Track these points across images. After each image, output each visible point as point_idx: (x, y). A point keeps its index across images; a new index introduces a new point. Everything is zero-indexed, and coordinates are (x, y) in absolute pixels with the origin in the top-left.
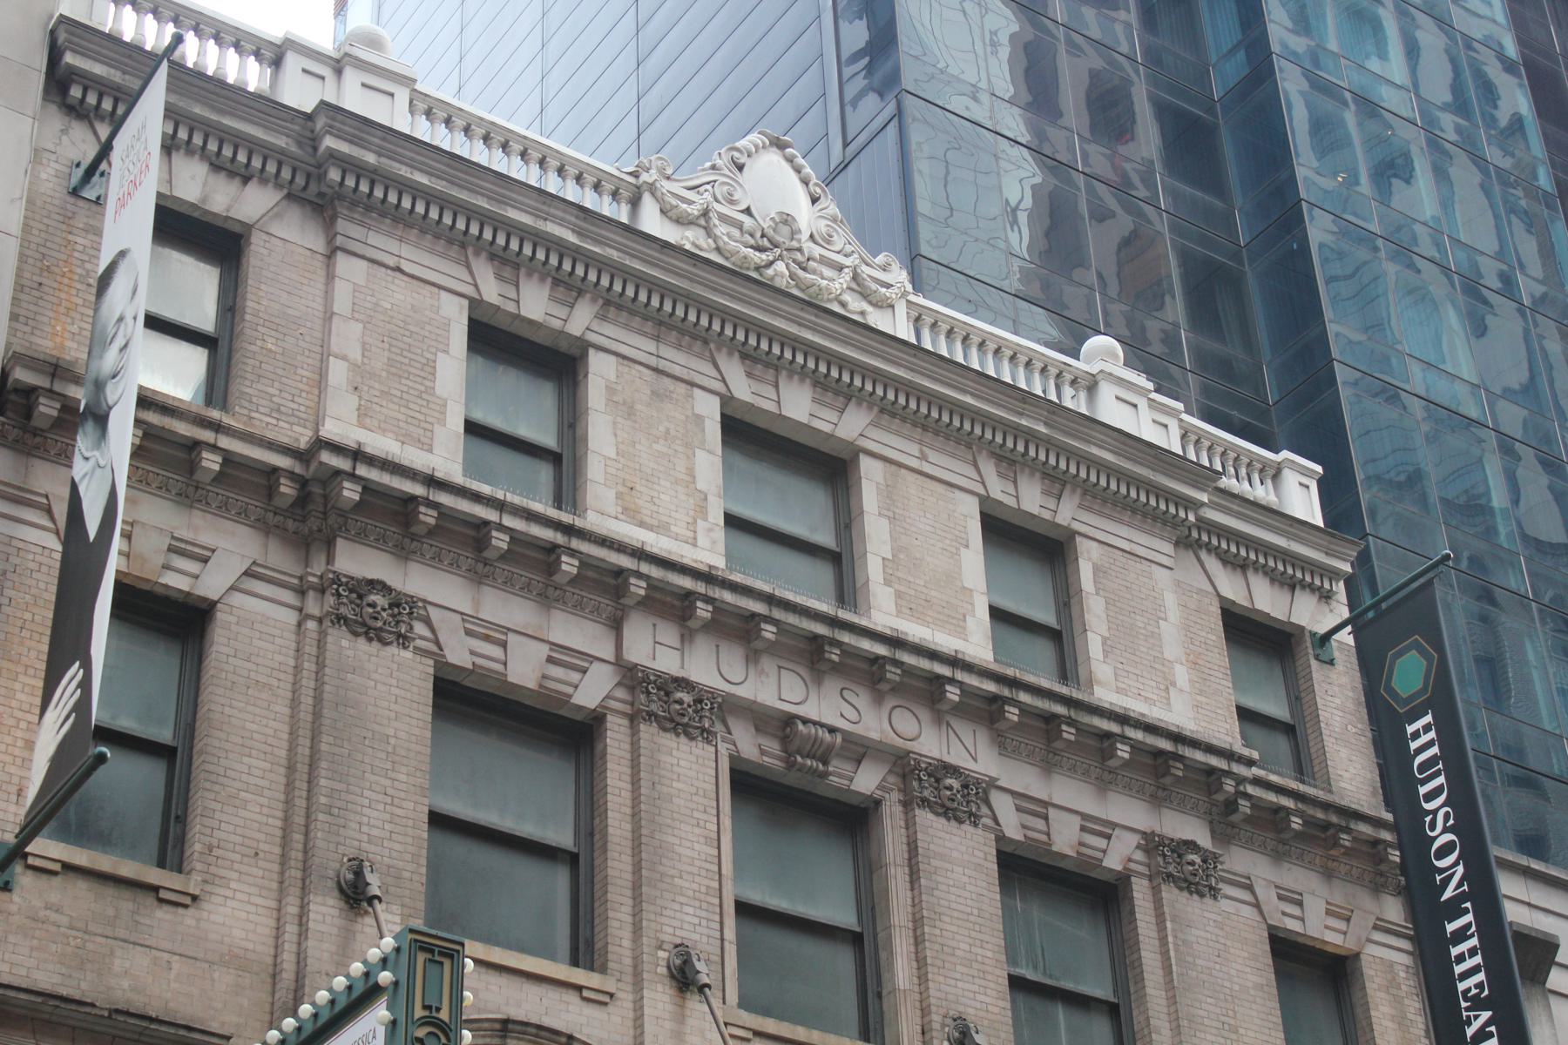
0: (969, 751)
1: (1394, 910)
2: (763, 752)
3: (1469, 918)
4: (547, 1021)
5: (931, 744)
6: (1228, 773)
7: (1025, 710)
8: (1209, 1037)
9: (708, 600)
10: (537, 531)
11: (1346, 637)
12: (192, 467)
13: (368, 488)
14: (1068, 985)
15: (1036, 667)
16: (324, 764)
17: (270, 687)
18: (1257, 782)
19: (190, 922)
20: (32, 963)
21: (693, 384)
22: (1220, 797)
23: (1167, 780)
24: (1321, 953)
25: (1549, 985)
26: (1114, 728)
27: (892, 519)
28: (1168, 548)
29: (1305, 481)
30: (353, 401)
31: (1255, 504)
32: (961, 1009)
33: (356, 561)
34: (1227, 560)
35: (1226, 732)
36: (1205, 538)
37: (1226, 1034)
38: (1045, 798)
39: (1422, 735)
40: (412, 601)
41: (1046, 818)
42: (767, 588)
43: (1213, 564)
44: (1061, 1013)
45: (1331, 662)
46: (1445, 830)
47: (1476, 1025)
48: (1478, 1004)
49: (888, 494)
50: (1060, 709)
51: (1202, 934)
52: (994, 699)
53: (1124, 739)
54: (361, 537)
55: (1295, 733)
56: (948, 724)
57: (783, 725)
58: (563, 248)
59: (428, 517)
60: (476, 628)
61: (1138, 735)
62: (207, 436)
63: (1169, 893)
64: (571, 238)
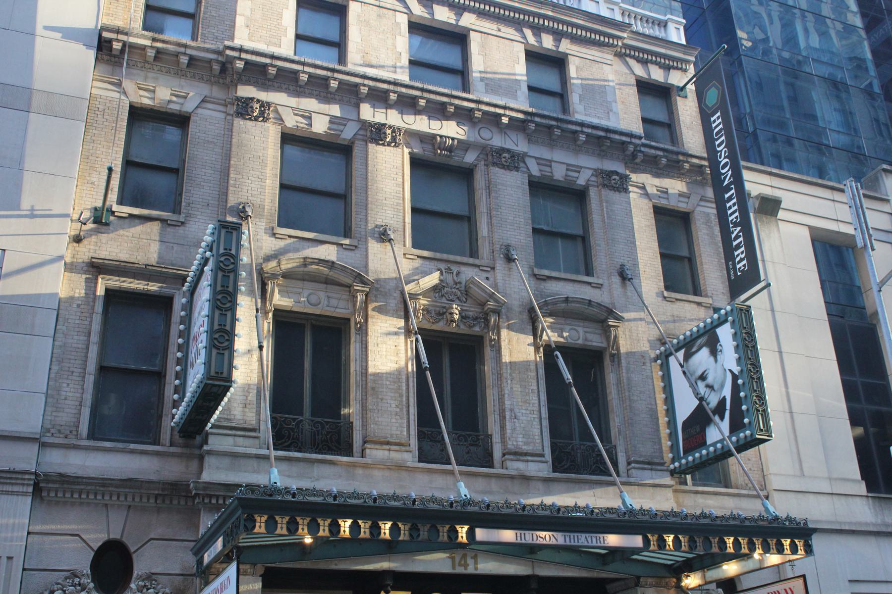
0: (517, 144)
1: (710, 193)
3: (733, 191)
4: (323, 258)
5: (497, 141)
6: (630, 143)
7: (537, 124)
9: (395, 92)
10: (319, 72)
11: (691, 87)
12: (178, 63)
13: (247, 62)
14: (564, 231)
15: (550, 107)
16: (232, 169)
17: (213, 142)
18: (644, 145)
20: (118, 251)
21: (395, 11)
22: (628, 153)
23: (604, 148)
24: (678, 212)
25: (778, 217)
26: (578, 128)
27: (485, 56)
28: (610, 57)
29: (678, 26)
30: (247, 31)
31: (649, 36)
33: (246, 91)
34: (639, 60)
35: (638, 128)
36: (628, 52)
38: (549, 158)
39: (717, 120)
40: (269, 104)
42: (420, 85)
43: (632, 62)
44: (559, 242)
45: (686, 97)
46: (725, 158)
47: (735, 233)
48: (736, 225)
49: (483, 46)
50: (554, 123)
52: (523, 121)
53: (582, 132)
54: (248, 83)
55: (670, 126)
59: (272, 71)
60: (296, 112)
61: (589, 131)
62: (182, 50)
63: (605, 192)
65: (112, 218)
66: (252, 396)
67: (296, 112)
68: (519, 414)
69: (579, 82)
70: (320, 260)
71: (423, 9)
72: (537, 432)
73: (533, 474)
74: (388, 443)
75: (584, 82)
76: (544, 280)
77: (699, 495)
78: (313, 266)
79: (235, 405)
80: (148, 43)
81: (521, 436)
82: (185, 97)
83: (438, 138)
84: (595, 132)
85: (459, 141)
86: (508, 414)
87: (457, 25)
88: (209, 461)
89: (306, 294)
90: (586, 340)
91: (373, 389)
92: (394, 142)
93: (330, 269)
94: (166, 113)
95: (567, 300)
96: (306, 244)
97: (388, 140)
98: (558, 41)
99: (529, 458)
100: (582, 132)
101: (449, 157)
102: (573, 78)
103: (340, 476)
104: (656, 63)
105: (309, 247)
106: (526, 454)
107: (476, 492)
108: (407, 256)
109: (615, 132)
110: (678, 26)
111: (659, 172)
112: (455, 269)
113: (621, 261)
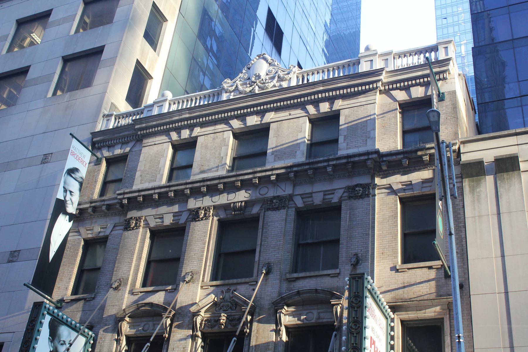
5: (271, 193)
8: (357, 240)
9: (204, 186)
13: (129, 199)
19: (92, 303)
25: (522, 169)
26: (326, 164)
32: (269, 261)
34: (401, 89)
37: (364, 237)
38: (310, 191)
40: (140, 218)
41: (312, 197)
50: (307, 167)
51: (361, 210)
57: (226, 207)
58: (187, 119)
60: (156, 217)
61: (334, 162)
62: (103, 203)
64: (187, 116)
65: (63, 304)
67: (156, 217)
69: (346, 125)
70: (145, 303)
71: (241, 123)
76: (294, 281)
78: (143, 308)
80: (87, 206)
82: (106, 228)
83: (232, 205)
84: (338, 162)
85: (246, 202)
87: (261, 124)
89: (143, 324)
90: (319, 318)
92: (206, 217)
94: (100, 239)
95: (298, 293)
96: (149, 294)
97: (201, 217)
98: (332, 104)
100: (329, 165)
101: (241, 214)
104: (416, 85)
105: (150, 296)
108: (204, 287)
109: (354, 156)
110: (446, 46)
112: (232, 288)
113: (354, 252)
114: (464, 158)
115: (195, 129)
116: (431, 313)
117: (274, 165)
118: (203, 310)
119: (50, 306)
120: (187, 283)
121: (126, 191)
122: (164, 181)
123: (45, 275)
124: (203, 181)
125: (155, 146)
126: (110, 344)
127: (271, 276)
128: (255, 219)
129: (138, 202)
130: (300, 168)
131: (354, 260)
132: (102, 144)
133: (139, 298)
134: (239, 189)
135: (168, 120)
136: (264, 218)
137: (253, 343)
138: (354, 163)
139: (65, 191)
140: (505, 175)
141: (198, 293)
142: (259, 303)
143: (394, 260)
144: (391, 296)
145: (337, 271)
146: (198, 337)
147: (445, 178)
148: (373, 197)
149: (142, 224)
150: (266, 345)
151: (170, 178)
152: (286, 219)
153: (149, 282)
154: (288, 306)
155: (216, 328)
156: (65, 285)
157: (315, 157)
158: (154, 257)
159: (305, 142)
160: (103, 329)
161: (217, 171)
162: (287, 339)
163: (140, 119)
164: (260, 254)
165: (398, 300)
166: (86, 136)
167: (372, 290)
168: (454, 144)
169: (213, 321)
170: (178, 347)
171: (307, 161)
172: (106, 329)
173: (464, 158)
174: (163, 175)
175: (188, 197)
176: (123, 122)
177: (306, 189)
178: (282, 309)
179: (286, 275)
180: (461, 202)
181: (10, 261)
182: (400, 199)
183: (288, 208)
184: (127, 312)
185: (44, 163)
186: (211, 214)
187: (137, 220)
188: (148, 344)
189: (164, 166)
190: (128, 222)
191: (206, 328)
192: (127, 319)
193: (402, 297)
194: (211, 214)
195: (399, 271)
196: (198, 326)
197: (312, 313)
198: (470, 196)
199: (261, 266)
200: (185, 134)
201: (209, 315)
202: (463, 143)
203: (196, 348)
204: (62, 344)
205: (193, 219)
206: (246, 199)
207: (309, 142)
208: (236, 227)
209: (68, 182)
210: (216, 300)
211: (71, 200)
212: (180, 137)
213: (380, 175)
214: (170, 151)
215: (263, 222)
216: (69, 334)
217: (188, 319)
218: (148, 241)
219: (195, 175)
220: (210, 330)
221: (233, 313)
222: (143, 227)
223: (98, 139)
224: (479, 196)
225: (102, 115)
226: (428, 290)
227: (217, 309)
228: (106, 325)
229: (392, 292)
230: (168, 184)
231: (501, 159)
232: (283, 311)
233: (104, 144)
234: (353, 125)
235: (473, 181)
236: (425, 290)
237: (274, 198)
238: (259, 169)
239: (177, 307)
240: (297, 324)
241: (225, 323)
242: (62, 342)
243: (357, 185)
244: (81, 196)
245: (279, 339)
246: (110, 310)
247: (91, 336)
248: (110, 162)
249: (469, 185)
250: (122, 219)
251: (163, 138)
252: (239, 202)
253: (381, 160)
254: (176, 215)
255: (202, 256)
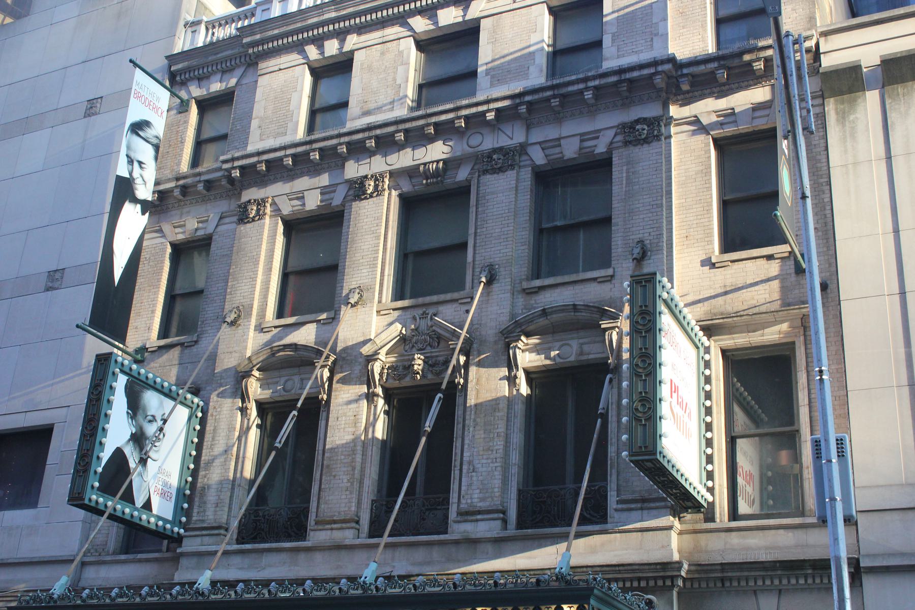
2: (414, 186)
5: (488, 142)
7: (530, 104)
8: (641, 217)
9: (370, 138)
13: (242, 168)
14: (585, 218)
19: (195, 350)
26: (581, 86)
38: (557, 136)
40: (264, 201)
41: (560, 146)
50: (549, 93)
51: (647, 163)
54: (250, 186)
56: (499, 129)
57: (411, 172)
60: (292, 196)
61: (597, 82)
62: (198, 179)
64: (333, 15)
65: (146, 354)
66: (226, 496)
67: (292, 196)
68: (487, 468)
69: (616, 15)
70: (284, 345)
71: (428, 22)
72: (497, 482)
73: (479, 536)
74: (335, 522)
75: (622, 13)
77: (734, 534)
78: (281, 354)
79: (209, 506)
80: (172, 185)
81: (478, 491)
82: (207, 221)
83: (422, 168)
84: (603, 81)
85: (445, 161)
86: (465, 467)
87: (464, 22)
88: (184, 562)
89: (283, 380)
90: (581, 353)
91: (328, 466)
92: (378, 191)
93: (295, 351)
94: (199, 240)
95: (544, 313)
96: (288, 330)
97: (369, 192)
99: (479, 517)
100: (587, 89)
101: (437, 183)
102: (607, 15)
103: (284, 563)
106: (480, 512)
107: (413, 564)
108: (382, 313)
109: (632, 69)
111: (723, 88)
112: (431, 311)
113: (637, 237)
114: (827, 62)
115: (349, 37)
116: (772, 334)
117: (491, 93)
118: (383, 351)
119: (124, 359)
120: (353, 306)
121: (236, 155)
122: (300, 133)
123: (111, 309)
124: (369, 128)
125: (281, 73)
126: (231, 417)
127: (496, 286)
128: (463, 191)
129: (259, 172)
130: (536, 97)
131: (637, 251)
132: (187, 76)
133: (273, 336)
134: (431, 140)
135: (299, 25)
136: (478, 187)
137: (471, 401)
138: (631, 81)
139: (131, 161)
140: (900, 89)
141: (372, 322)
142: (478, 333)
143: (707, 247)
144: (703, 309)
145: (610, 272)
146: (378, 395)
147: (793, 99)
148: (668, 141)
149: (268, 210)
150: (494, 402)
151: (311, 127)
152: (517, 186)
153: (288, 309)
154: (528, 335)
155: (408, 379)
156: (146, 322)
157: (562, 75)
158: (293, 265)
159: (542, 49)
160: (216, 392)
161: (392, 109)
162: (529, 392)
163: (250, 25)
164: (475, 250)
165: (715, 315)
166: (158, 62)
167: (669, 301)
168: (807, 38)
169: (402, 368)
170: (345, 415)
171: (549, 83)
172: (222, 392)
173: (827, 62)
174: (297, 122)
175: (344, 159)
176: (222, 33)
177: (549, 132)
178: (517, 341)
179: (521, 283)
180: (823, 141)
181: (48, 289)
182: (715, 141)
183: (520, 167)
184: (255, 362)
185: (89, 116)
186: (386, 187)
187: (259, 204)
188: (295, 413)
189: (299, 108)
190: (244, 208)
191: (390, 381)
192: (256, 373)
193: (722, 309)
194: (386, 187)
195: (717, 265)
196: (377, 377)
197: (568, 345)
198: (837, 129)
199: (478, 270)
200: (332, 47)
201: (394, 359)
202: (825, 34)
203: (375, 414)
204: (150, 421)
205: (355, 197)
206: (444, 156)
207: (551, 49)
208: (431, 205)
209: (133, 146)
210: (404, 332)
211: (142, 176)
212: (322, 53)
213: (678, 100)
214: (308, 79)
215: (478, 194)
216: (161, 403)
217: (360, 367)
218: (280, 240)
219: (355, 119)
220: (396, 384)
221: (435, 352)
222: (271, 216)
223: (180, 66)
224: (853, 128)
225: (182, 23)
226: (767, 296)
227: (407, 347)
228: (221, 385)
229: (706, 303)
230: (308, 139)
231: (891, 60)
232: (520, 344)
233: (192, 75)
234: (627, 14)
235: (843, 103)
236: (760, 297)
237: (495, 150)
238: (465, 102)
239: (338, 349)
240: (544, 366)
241: (422, 371)
242: (150, 418)
243: (638, 121)
244: (159, 169)
245: (515, 392)
246: (226, 360)
247: (198, 406)
248: (204, 105)
249: (836, 109)
250: (234, 204)
251: (293, 58)
252: (433, 162)
253: (679, 73)
254: (325, 191)
255: (376, 258)
